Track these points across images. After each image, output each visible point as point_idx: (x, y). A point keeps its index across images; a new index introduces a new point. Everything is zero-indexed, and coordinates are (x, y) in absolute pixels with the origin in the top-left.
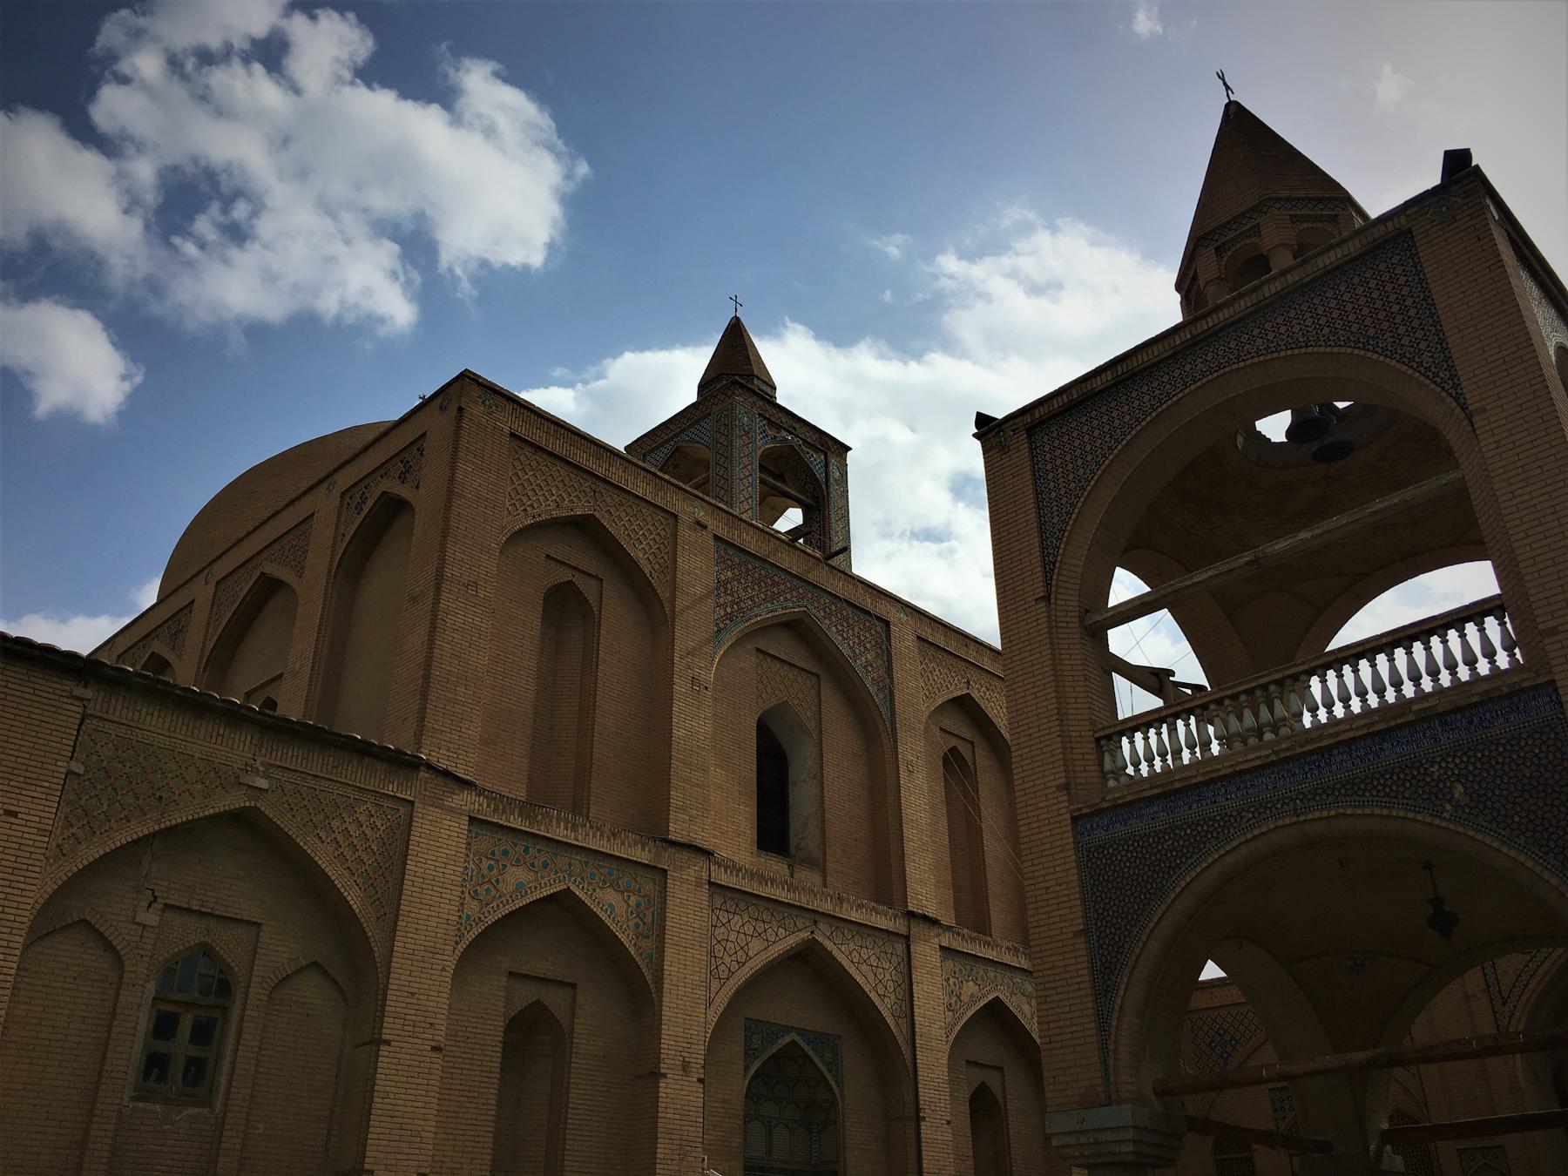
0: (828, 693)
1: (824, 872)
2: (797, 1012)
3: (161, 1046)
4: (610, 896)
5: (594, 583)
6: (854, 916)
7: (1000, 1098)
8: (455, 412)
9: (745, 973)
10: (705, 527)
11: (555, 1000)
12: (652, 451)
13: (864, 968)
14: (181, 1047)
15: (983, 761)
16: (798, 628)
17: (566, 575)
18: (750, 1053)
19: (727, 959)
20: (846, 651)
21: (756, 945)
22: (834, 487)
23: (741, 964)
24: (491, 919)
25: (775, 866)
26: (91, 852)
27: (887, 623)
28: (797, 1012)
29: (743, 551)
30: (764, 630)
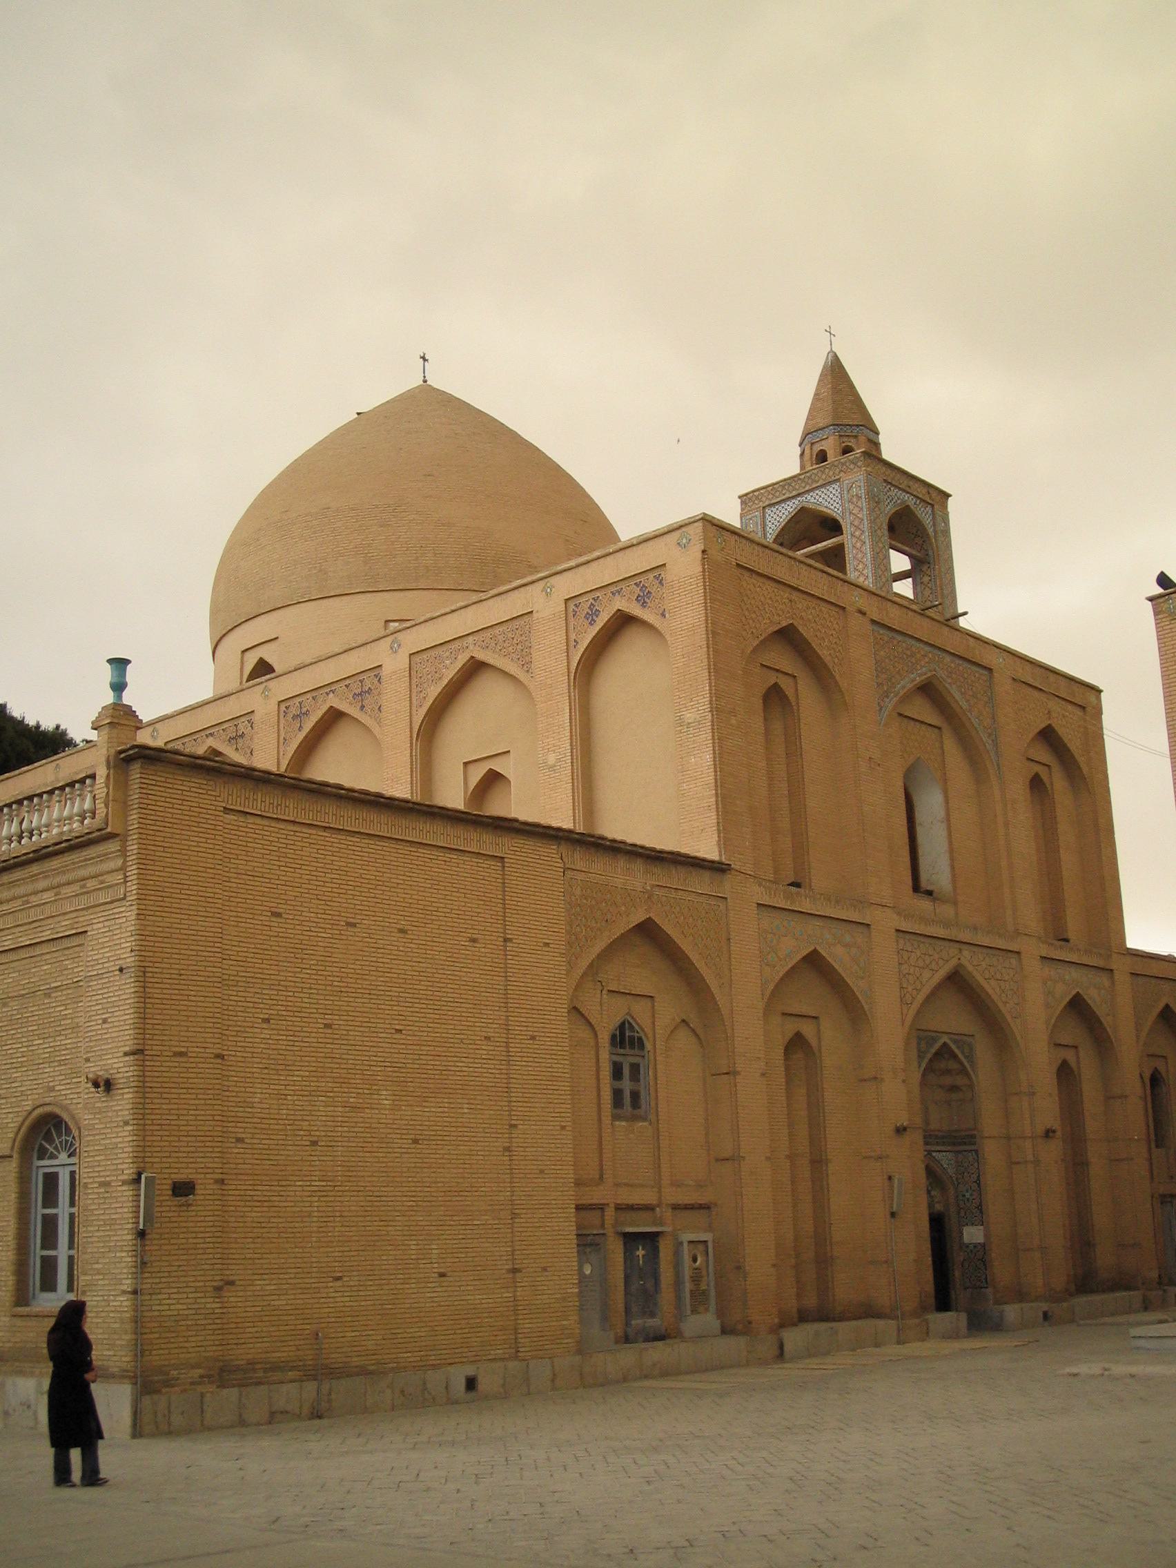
0: (950, 744)
1: (955, 903)
2: (953, 1020)
3: (618, 1084)
4: (839, 950)
5: (790, 680)
6: (986, 941)
7: (1075, 1069)
8: (699, 555)
9: (920, 998)
10: (864, 614)
11: (808, 1030)
12: (770, 505)
13: (993, 982)
14: (626, 1085)
15: (1058, 783)
16: (928, 690)
17: (773, 678)
18: (920, 1057)
19: (910, 989)
20: (965, 705)
21: (927, 974)
22: (941, 539)
23: (919, 991)
24: (777, 978)
25: (925, 904)
26: (584, 964)
27: (990, 670)
28: (953, 1020)
29: (890, 628)
30: (905, 699)
